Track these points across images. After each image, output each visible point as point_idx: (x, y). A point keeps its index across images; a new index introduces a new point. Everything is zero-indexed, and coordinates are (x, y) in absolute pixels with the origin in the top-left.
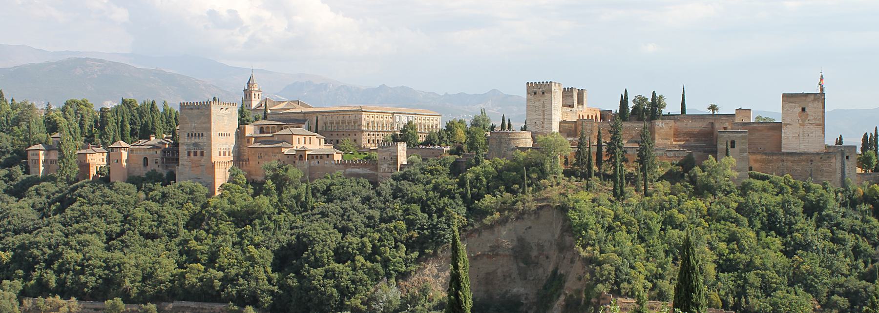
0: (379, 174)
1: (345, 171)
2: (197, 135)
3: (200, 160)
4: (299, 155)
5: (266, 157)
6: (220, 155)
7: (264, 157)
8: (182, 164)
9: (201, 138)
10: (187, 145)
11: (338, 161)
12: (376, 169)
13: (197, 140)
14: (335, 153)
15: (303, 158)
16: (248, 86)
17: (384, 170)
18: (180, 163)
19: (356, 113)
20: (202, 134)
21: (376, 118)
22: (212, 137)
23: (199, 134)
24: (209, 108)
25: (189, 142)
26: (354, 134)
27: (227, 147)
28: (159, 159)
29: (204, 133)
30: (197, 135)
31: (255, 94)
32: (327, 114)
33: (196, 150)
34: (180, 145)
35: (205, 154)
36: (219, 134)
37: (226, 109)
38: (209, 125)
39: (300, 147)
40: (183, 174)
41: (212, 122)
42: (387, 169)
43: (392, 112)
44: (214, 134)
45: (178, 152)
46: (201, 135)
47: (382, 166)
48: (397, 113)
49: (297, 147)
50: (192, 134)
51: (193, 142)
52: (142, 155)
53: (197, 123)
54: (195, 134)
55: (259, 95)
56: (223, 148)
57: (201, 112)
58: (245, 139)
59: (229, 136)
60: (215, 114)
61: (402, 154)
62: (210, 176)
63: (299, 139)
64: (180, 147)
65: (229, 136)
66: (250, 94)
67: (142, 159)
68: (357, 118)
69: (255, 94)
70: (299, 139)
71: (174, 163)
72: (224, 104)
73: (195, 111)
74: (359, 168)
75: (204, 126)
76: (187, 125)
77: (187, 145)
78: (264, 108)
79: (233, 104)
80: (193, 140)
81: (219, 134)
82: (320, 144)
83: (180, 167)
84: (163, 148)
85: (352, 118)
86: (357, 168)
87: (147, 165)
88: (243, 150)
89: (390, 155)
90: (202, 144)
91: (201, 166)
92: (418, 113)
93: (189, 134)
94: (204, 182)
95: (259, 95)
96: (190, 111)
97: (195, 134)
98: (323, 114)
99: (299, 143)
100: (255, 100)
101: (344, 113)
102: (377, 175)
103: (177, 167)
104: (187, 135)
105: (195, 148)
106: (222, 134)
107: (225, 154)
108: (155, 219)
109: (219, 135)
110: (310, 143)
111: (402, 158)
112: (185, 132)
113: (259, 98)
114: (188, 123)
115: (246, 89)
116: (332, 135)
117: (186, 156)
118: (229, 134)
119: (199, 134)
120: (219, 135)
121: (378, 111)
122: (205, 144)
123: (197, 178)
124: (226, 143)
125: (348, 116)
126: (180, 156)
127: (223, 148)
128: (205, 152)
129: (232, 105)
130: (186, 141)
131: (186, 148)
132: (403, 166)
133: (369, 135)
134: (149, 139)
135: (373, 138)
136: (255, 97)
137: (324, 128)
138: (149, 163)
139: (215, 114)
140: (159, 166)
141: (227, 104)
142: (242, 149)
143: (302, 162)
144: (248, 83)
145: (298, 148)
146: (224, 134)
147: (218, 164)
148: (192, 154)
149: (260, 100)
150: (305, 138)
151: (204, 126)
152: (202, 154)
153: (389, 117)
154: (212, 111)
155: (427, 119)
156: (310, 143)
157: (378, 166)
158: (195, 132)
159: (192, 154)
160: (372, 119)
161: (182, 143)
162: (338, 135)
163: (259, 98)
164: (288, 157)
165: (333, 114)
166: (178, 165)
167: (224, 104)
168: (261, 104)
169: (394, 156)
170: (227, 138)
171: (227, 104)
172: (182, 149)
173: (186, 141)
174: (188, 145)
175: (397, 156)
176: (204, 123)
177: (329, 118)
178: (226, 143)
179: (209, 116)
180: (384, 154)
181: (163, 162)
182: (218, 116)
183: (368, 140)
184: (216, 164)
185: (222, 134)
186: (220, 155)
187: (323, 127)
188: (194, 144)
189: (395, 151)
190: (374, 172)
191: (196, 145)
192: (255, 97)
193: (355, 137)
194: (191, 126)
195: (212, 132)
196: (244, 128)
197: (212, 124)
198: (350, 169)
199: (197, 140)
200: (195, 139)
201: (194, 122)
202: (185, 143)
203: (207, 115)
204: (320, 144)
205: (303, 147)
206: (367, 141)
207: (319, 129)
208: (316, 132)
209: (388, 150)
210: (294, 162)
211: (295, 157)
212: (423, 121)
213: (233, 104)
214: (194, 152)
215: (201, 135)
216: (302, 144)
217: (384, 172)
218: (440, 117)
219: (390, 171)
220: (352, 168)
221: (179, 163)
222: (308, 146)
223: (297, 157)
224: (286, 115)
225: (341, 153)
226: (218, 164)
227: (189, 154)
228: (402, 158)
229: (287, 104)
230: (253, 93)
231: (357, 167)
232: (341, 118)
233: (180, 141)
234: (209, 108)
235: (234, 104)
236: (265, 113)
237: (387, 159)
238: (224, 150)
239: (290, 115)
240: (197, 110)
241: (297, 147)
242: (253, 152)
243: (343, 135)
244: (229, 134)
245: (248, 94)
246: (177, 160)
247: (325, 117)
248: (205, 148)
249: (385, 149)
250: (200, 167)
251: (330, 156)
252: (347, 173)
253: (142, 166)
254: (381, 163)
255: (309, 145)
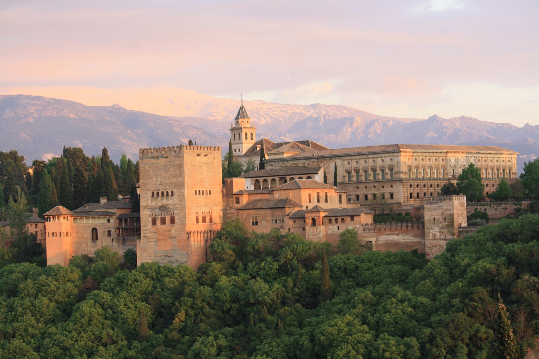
0: (428, 243)
1: (377, 240)
2: (165, 194)
3: (169, 229)
4: (311, 218)
5: (264, 223)
6: (197, 221)
7: (261, 223)
8: (144, 236)
9: (170, 198)
10: (150, 208)
11: (367, 224)
12: (423, 235)
13: (165, 202)
14: (363, 215)
15: (317, 223)
16: (237, 123)
17: (435, 235)
18: (142, 235)
19: (391, 154)
20: (172, 192)
21: (421, 160)
22: (186, 196)
23: (167, 193)
24: (180, 155)
25: (153, 204)
26: (389, 186)
27: (206, 209)
28: (113, 231)
29: (175, 191)
30: (165, 194)
31: (246, 134)
32: (349, 158)
33: (163, 216)
34: (141, 209)
35: (176, 221)
36: (196, 191)
37: (206, 155)
38: (181, 179)
39: (311, 206)
40: (146, 251)
41: (186, 175)
42: (438, 234)
43: (445, 151)
44: (188, 192)
45: (138, 220)
46: (170, 194)
47: (431, 231)
48: (451, 152)
49: (307, 207)
50: (158, 193)
51: (160, 204)
52: (89, 225)
53: (164, 177)
54: (163, 193)
55: (252, 134)
56: (202, 211)
57: (170, 162)
58: (233, 198)
59: (210, 194)
60: (189, 164)
61: (460, 212)
62: (185, 252)
63: (310, 195)
64: (142, 213)
65: (210, 194)
66: (239, 134)
67: (90, 231)
68: (394, 163)
69: (246, 134)
70: (310, 195)
71: (134, 235)
72: (202, 149)
73: (162, 161)
74: (398, 235)
75: (175, 180)
76: (151, 180)
77: (150, 208)
78: (260, 152)
79: (215, 148)
80: (160, 202)
81: (196, 191)
82: (340, 201)
83: (142, 240)
84: (118, 215)
85: (387, 161)
86: (394, 234)
87: (97, 239)
88: (231, 213)
89: (443, 214)
90: (172, 207)
91: (171, 238)
92: (482, 152)
93: (153, 193)
94: (176, 260)
95: (252, 134)
96: (154, 161)
97: (163, 193)
98: (344, 158)
99: (310, 202)
100: (247, 141)
101: (375, 156)
102: (424, 244)
103: (138, 241)
104: (150, 195)
105: (163, 213)
106: (199, 191)
107: (204, 221)
108: (107, 315)
109: (196, 194)
110: (326, 201)
111: (460, 217)
112: (147, 190)
113: (252, 139)
114: (152, 178)
115: (234, 126)
116: (358, 188)
117: (151, 224)
118: (210, 191)
119: (167, 193)
120: (196, 194)
121: (423, 151)
122: (177, 206)
123: (166, 256)
124: (206, 205)
125: (380, 159)
126: (141, 225)
127: (202, 211)
128: (176, 217)
129: (212, 149)
130: (150, 202)
131: (150, 213)
132: (461, 229)
133: (411, 186)
134: (98, 201)
135: (417, 190)
136: (246, 138)
137: (347, 179)
138: (99, 236)
139: (189, 164)
140: (113, 239)
141: (206, 149)
142: (229, 212)
143: (315, 228)
144: (237, 118)
145: (309, 209)
146: (203, 191)
147: (196, 234)
148: (158, 222)
149: (254, 141)
150: (318, 193)
151: (175, 180)
152: (173, 221)
153: (441, 158)
154: (185, 159)
155: (496, 159)
156: (326, 201)
157: (426, 230)
158: (161, 190)
159: (158, 222)
160: (415, 163)
161: (145, 206)
162: (366, 187)
163: (252, 139)
164: (295, 222)
165: (357, 157)
166: (139, 238)
167: (202, 149)
168: (256, 148)
169: (448, 215)
170: (207, 197)
171: (206, 149)
172: (145, 215)
173: (150, 202)
174: (152, 209)
175: (452, 215)
176: (174, 177)
177: (354, 164)
178: (206, 205)
179: (180, 167)
180: (434, 213)
181: (118, 235)
182: (193, 165)
183: (411, 194)
184: (192, 234)
185: (199, 191)
186: (197, 221)
187: (344, 177)
188: (160, 207)
189: (449, 207)
190: (419, 240)
191: (163, 208)
192: (246, 138)
193: (391, 190)
194: (156, 181)
195: (186, 189)
196: (232, 183)
197: (186, 177)
198: (385, 236)
199: (165, 202)
200: (162, 200)
201: (161, 175)
202: (148, 206)
203: (178, 165)
204: (340, 201)
205: (316, 206)
206: (409, 195)
207: (339, 180)
208: (335, 184)
209: (439, 207)
210: (304, 229)
211: (305, 221)
212: (490, 163)
213: (215, 148)
214: (161, 218)
215: (170, 194)
216: (314, 203)
217: (434, 239)
218: (516, 156)
219: (443, 236)
220: (388, 235)
221: (140, 234)
222: (323, 205)
223: (307, 221)
224: (291, 162)
225: (371, 213)
226: (196, 234)
227: (154, 222)
228: (460, 217)
229: (293, 145)
230: (244, 131)
231: (395, 232)
232: (370, 163)
233: (143, 203)
234: (180, 155)
235: (216, 149)
236: (261, 160)
237: (438, 220)
238: (204, 215)
239: (296, 162)
240: (164, 159)
241: (307, 207)
242: (245, 216)
243: (375, 187)
244: (210, 191)
245: (236, 131)
246: (136, 232)
247: (346, 162)
248: (175, 212)
249: (434, 205)
250: (170, 240)
251: (356, 219)
252: (380, 242)
253: (90, 240)
254: (429, 226)
255: (326, 203)
